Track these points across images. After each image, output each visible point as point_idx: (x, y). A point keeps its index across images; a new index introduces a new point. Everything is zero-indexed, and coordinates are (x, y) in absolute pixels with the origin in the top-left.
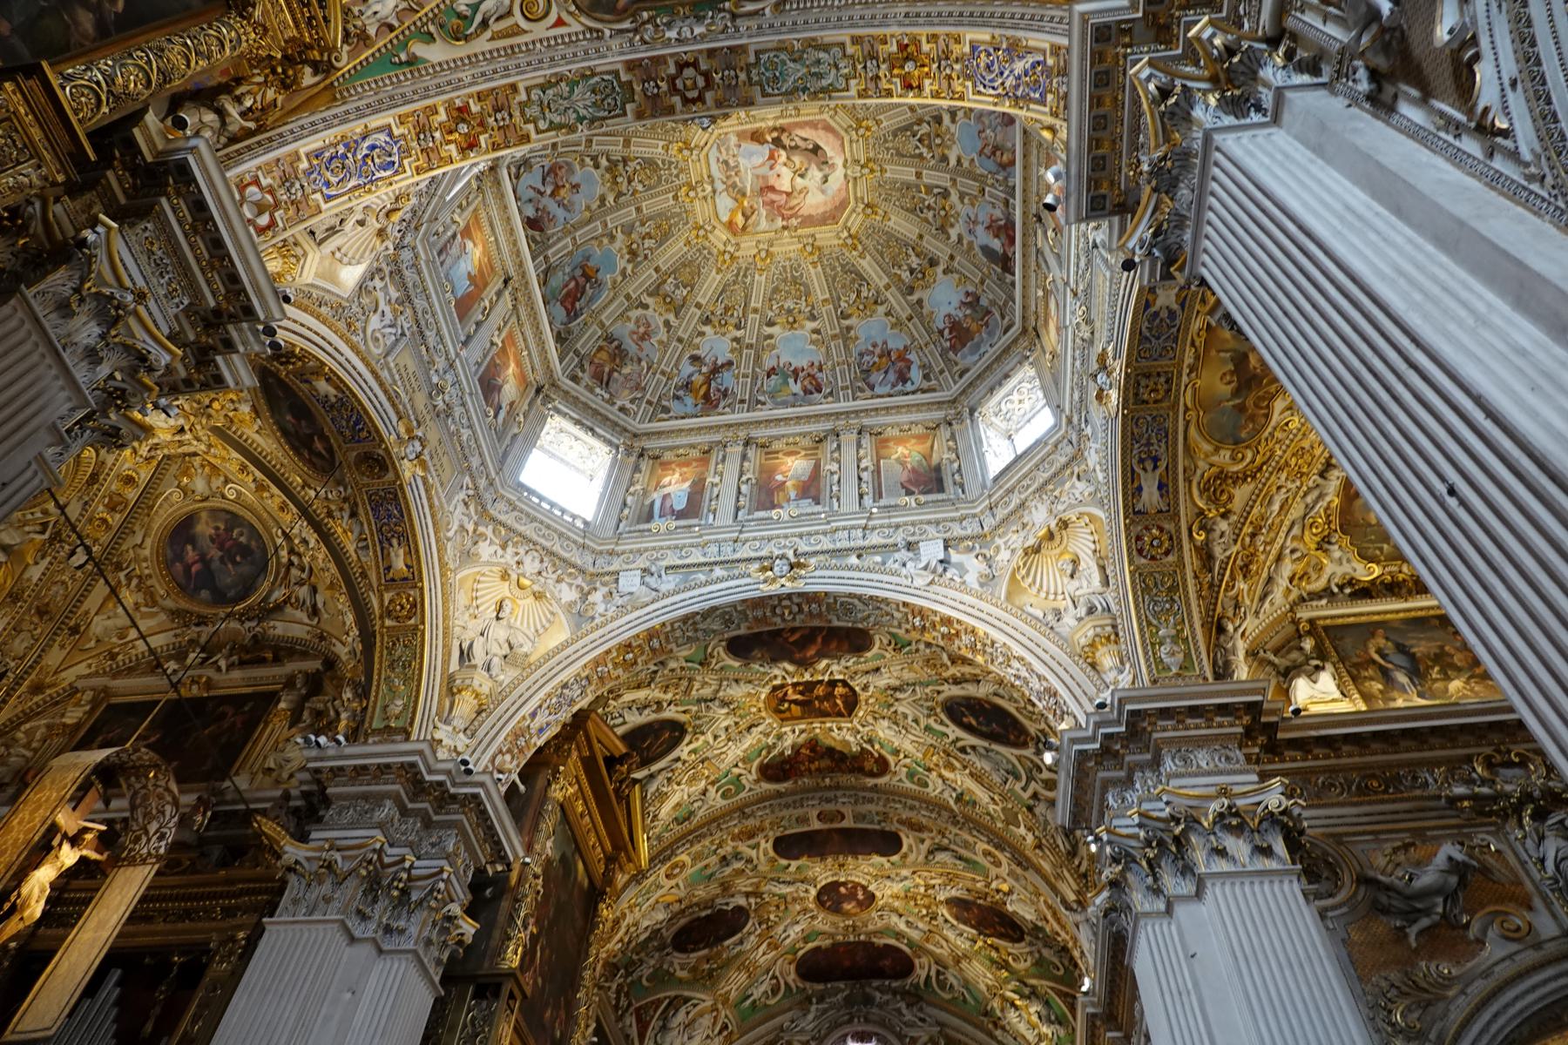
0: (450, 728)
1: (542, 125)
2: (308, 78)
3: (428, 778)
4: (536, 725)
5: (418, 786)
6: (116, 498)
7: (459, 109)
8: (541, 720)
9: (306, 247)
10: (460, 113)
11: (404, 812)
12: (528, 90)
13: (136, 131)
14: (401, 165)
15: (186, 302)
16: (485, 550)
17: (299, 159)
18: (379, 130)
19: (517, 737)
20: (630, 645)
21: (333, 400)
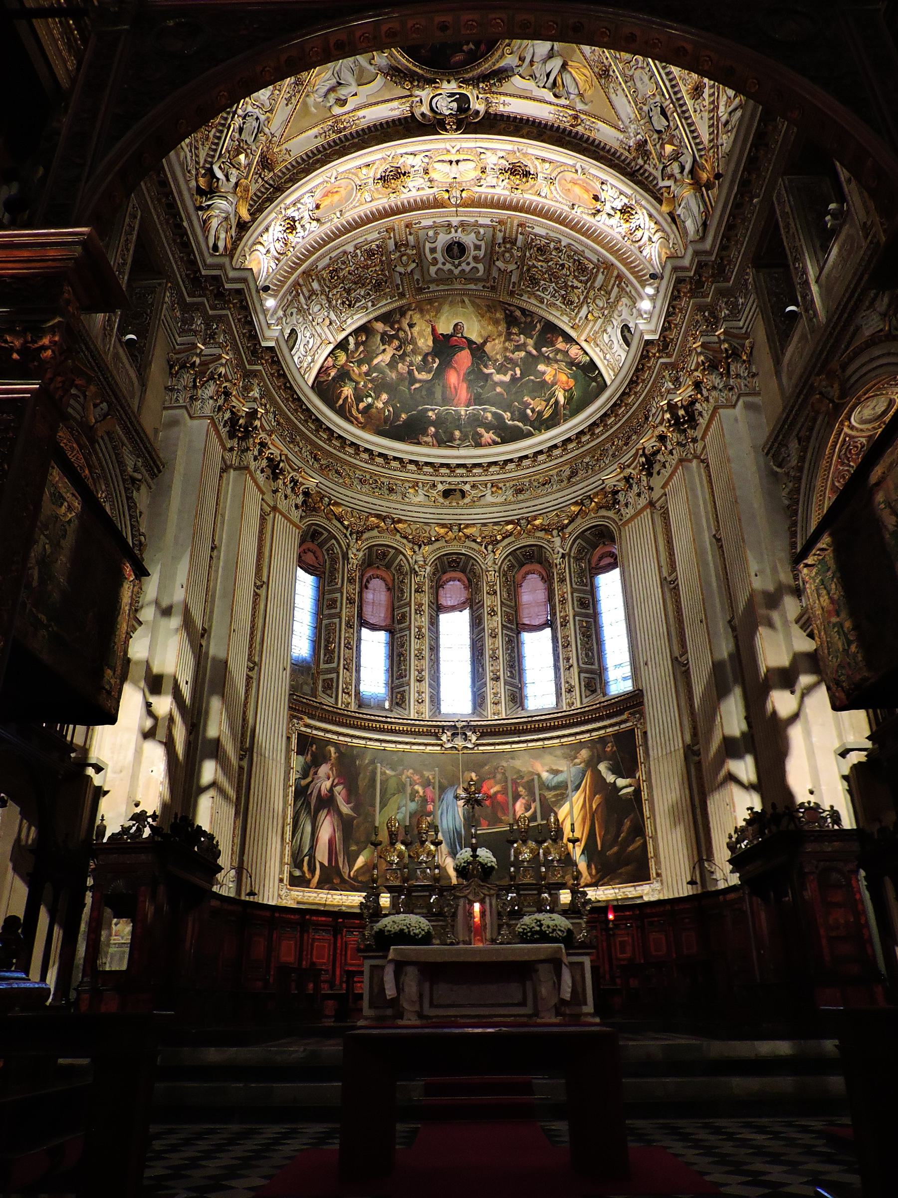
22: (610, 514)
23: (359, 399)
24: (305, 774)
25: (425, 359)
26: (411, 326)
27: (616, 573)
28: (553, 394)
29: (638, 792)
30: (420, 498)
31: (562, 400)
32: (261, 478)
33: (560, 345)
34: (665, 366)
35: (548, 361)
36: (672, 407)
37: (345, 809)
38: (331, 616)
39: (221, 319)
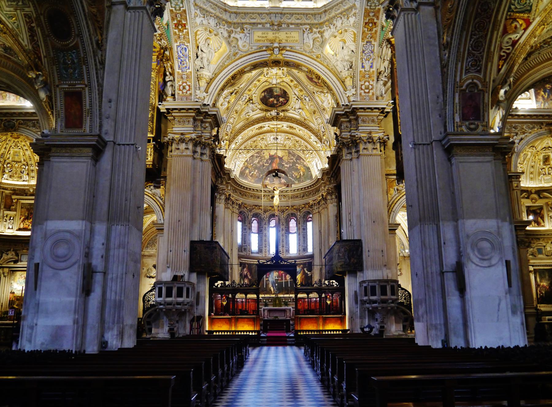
0: (348, 91)
1: (181, 6)
2: (167, 53)
3: (343, 113)
4: (367, 67)
5: (346, 115)
6: (295, 85)
7: (175, 26)
8: (367, 65)
9: (202, 73)
10: (177, 26)
11: (350, 121)
12: (172, 7)
13: (162, 111)
14: (186, 46)
15: (192, 120)
16: (326, 35)
17: (179, 72)
18: (177, 49)
19: (364, 77)
20: (366, 23)
21: (252, 67)
22: (311, 209)
23: (250, 173)
24: (242, 271)
25: (267, 160)
26: (263, 153)
27: (311, 222)
28: (300, 172)
29: (312, 275)
30: (266, 199)
31: (302, 174)
32: (231, 207)
33: (302, 161)
34: (323, 183)
35: (299, 164)
36: (322, 195)
37: (250, 277)
38: (245, 232)
39: (224, 178)
